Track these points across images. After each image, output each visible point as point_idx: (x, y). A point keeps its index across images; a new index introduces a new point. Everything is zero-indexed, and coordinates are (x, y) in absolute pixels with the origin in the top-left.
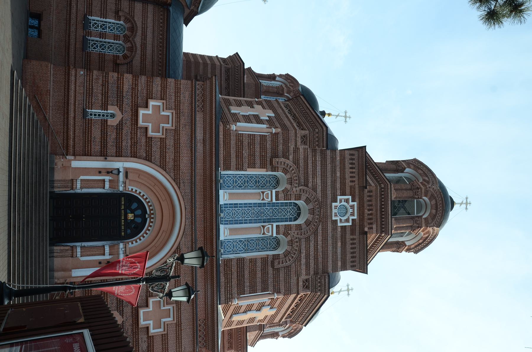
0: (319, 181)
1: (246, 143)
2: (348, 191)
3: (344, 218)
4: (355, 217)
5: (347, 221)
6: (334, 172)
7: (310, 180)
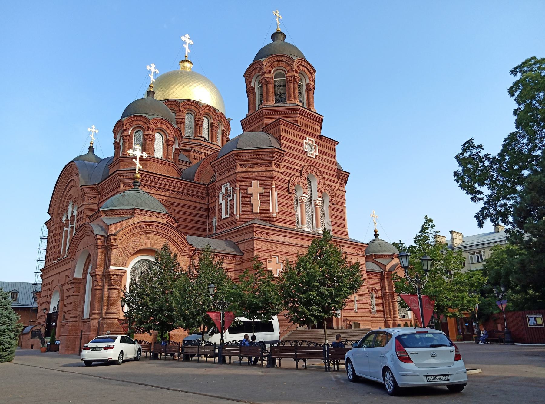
0: (297, 161)
1: (282, 208)
2: (301, 141)
3: (314, 150)
4: (314, 140)
5: (315, 147)
6: (291, 148)
7: (297, 168)
